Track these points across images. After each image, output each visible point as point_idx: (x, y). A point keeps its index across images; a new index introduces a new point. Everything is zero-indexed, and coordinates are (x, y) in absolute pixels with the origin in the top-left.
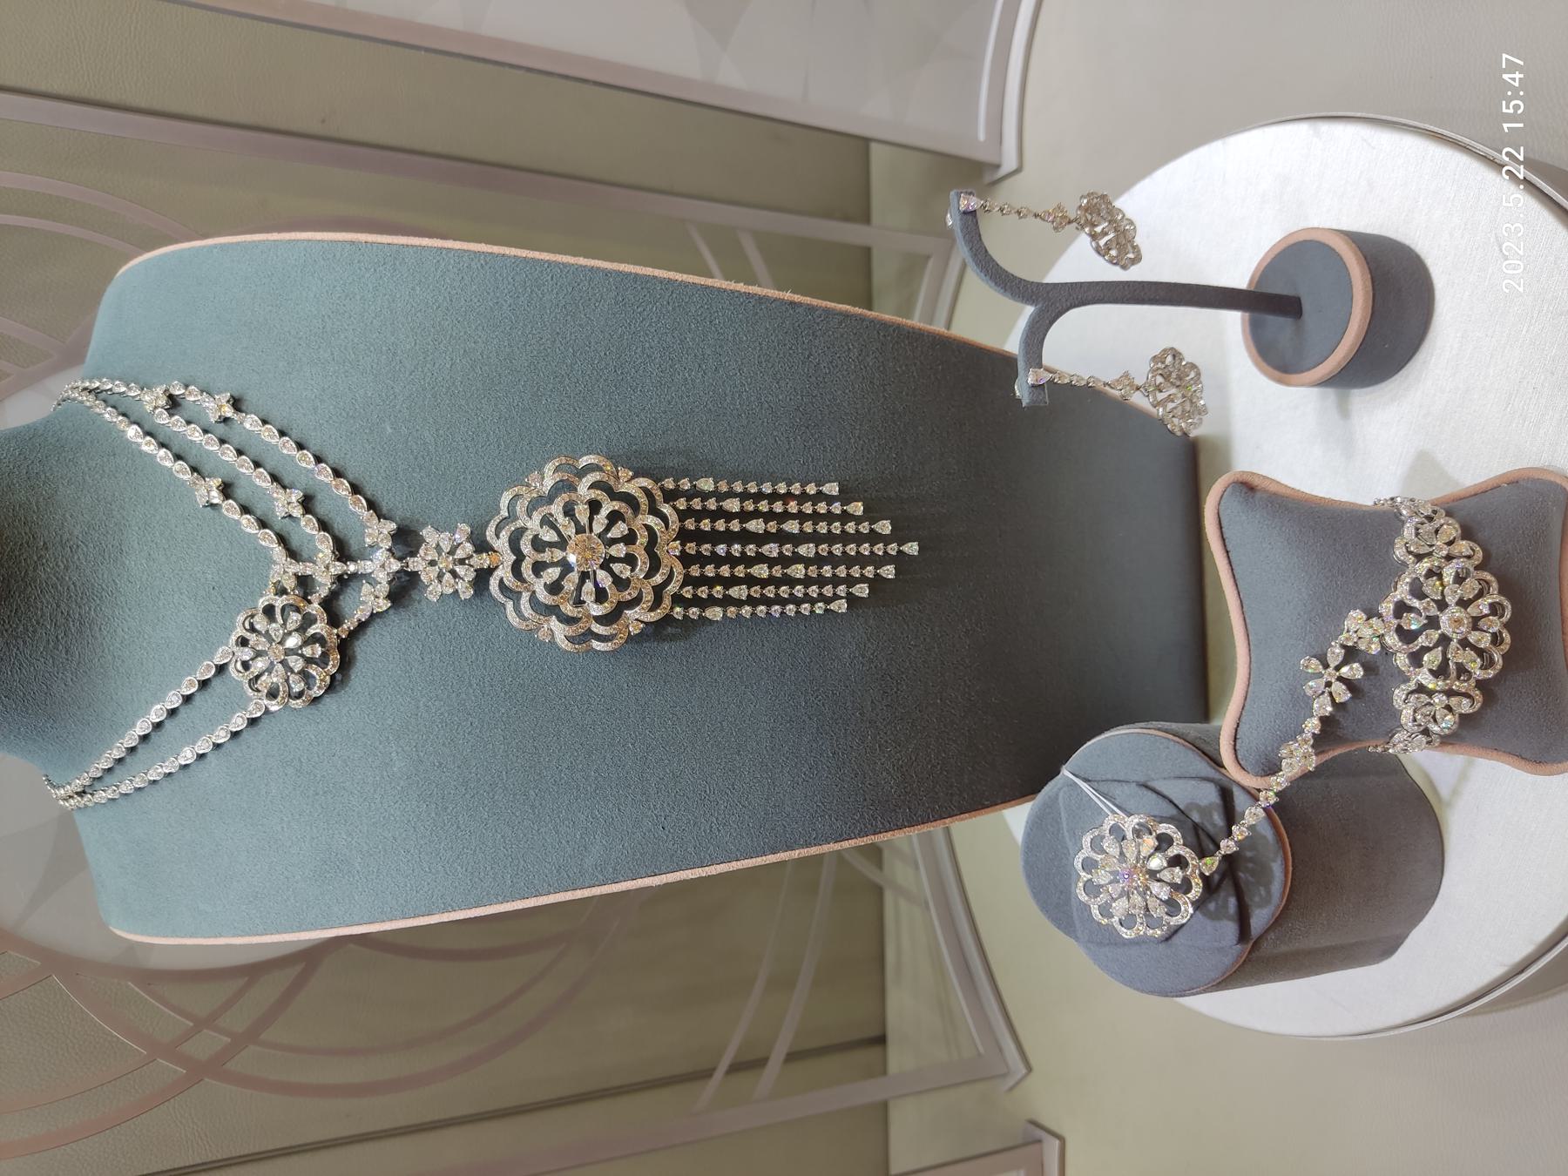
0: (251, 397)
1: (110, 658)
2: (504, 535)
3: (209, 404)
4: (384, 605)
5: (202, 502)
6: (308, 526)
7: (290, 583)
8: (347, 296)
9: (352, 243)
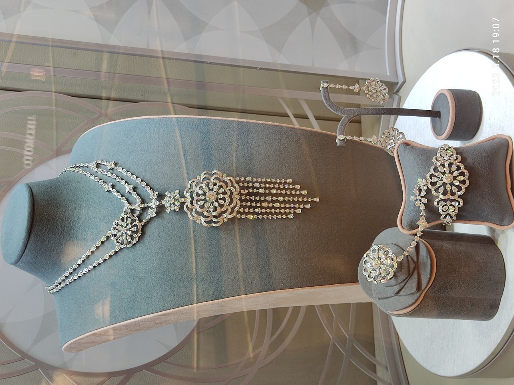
0: (119, 162)
1: (75, 238)
2: (189, 192)
3: (109, 165)
4: (154, 215)
5: (106, 190)
6: (134, 195)
7: (129, 211)
8: (146, 133)
9: (148, 119)
